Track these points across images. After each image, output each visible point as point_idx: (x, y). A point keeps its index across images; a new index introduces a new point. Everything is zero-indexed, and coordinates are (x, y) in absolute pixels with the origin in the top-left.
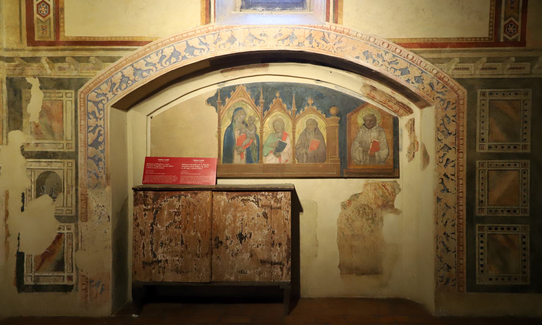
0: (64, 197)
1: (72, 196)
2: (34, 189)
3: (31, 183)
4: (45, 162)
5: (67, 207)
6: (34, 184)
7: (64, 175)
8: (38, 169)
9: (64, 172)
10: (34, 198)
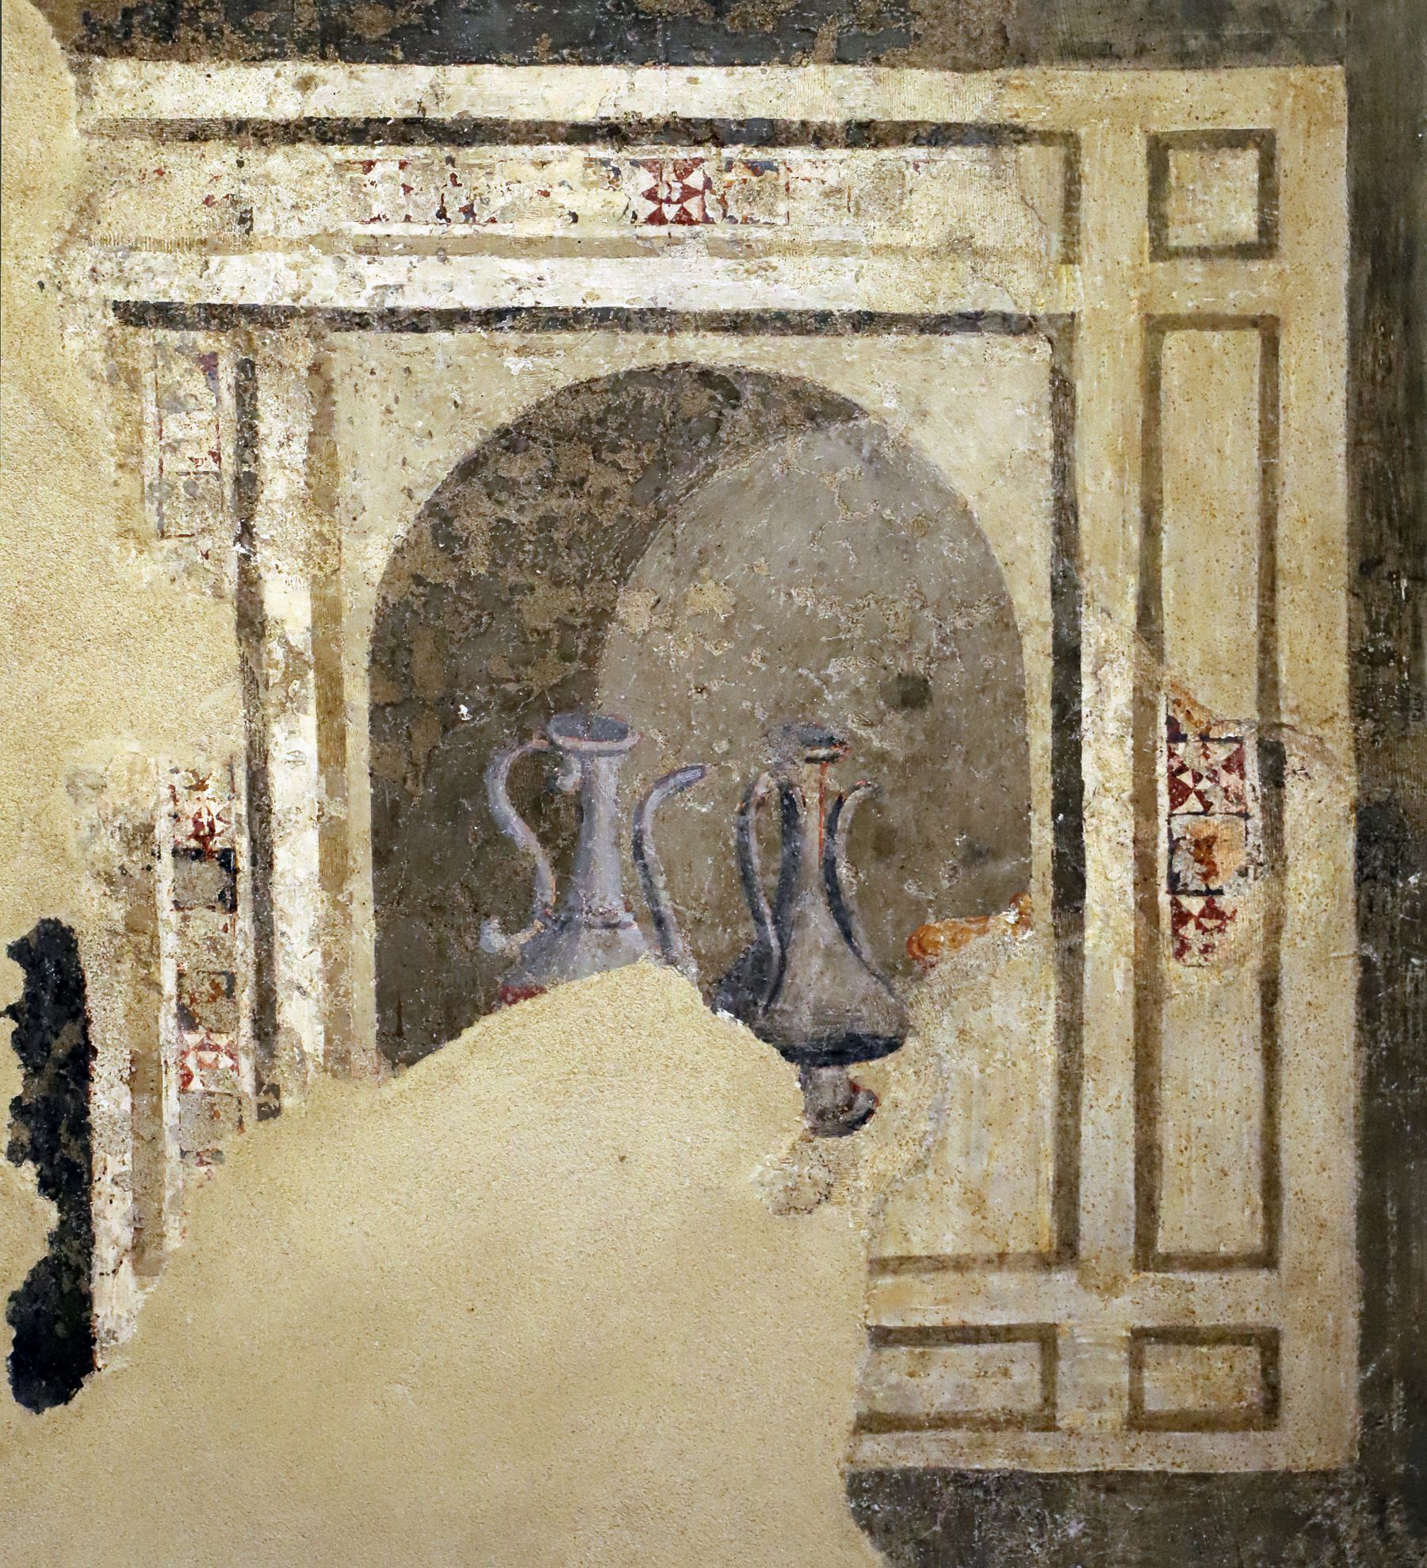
0: (1070, 1029)
1: (1270, 990)
2: (332, 837)
3: (253, 682)
4: (580, 134)
5: (1147, 1256)
6: (331, 708)
7: (1063, 473)
8: (418, 322)
9: (1062, 387)
10: (338, 1061)
